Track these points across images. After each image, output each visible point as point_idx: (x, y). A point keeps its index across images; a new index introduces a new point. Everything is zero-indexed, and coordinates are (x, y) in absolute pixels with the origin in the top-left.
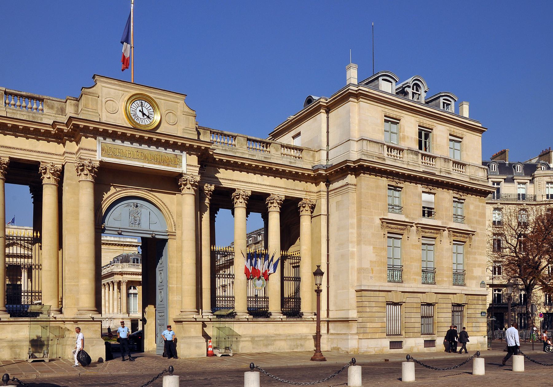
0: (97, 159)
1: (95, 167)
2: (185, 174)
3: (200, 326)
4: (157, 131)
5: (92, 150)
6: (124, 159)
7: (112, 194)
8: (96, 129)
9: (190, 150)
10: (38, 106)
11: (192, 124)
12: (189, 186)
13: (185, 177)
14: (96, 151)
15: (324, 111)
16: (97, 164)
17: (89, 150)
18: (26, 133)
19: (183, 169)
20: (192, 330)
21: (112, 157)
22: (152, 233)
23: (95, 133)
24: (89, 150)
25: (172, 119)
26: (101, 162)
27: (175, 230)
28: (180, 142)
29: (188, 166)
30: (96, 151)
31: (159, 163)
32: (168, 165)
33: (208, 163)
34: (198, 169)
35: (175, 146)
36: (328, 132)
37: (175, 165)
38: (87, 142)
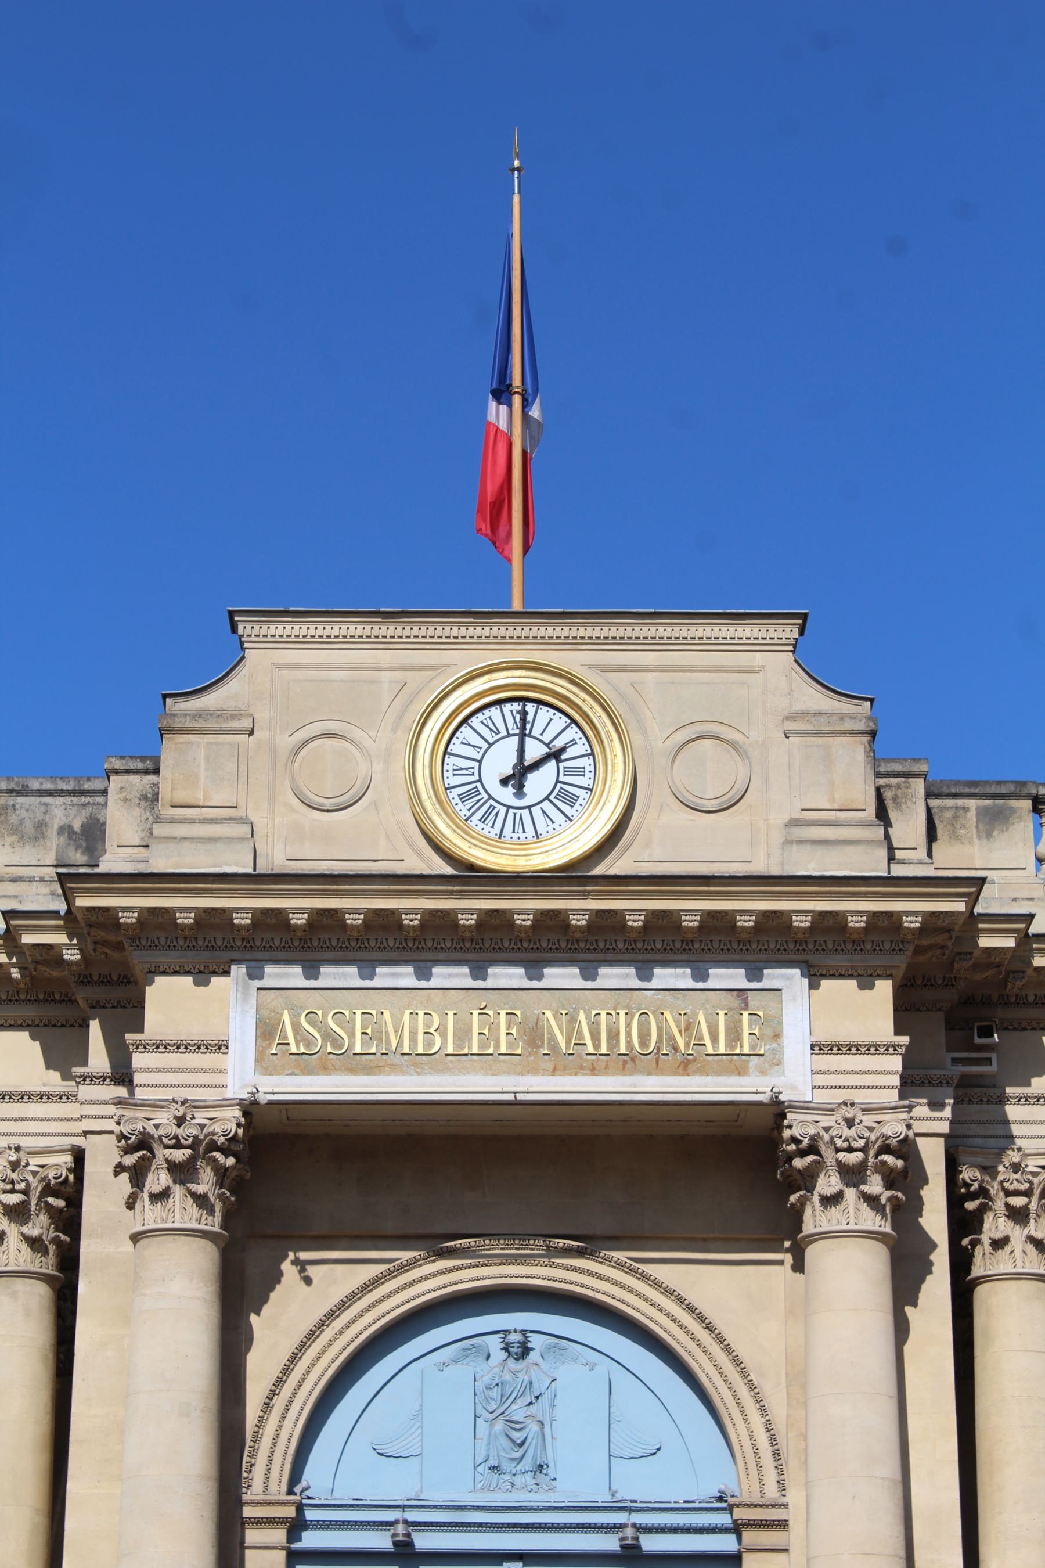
0: (230, 1095)
1: (213, 1146)
2: (794, 1106)
4: (613, 865)
5: (201, 1046)
6: (395, 1069)
7: (317, 1297)
8: (213, 921)
9: (824, 949)
11: (847, 774)
12: (829, 1183)
13: (799, 1126)
14: (222, 1046)
16: (228, 1122)
17: (180, 1046)
19: (791, 1075)
21: (325, 1068)
22: (620, 1518)
23: (213, 946)
24: (180, 1046)
25: (712, 773)
26: (250, 1109)
27: (782, 1486)
28: (747, 907)
29: (818, 1050)
30: (222, 1046)
31: (629, 1063)
32: (686, 1066)
34: (896, 1063)
35: (713, 942)
37: (734, 1063)
38: (171, 1002)
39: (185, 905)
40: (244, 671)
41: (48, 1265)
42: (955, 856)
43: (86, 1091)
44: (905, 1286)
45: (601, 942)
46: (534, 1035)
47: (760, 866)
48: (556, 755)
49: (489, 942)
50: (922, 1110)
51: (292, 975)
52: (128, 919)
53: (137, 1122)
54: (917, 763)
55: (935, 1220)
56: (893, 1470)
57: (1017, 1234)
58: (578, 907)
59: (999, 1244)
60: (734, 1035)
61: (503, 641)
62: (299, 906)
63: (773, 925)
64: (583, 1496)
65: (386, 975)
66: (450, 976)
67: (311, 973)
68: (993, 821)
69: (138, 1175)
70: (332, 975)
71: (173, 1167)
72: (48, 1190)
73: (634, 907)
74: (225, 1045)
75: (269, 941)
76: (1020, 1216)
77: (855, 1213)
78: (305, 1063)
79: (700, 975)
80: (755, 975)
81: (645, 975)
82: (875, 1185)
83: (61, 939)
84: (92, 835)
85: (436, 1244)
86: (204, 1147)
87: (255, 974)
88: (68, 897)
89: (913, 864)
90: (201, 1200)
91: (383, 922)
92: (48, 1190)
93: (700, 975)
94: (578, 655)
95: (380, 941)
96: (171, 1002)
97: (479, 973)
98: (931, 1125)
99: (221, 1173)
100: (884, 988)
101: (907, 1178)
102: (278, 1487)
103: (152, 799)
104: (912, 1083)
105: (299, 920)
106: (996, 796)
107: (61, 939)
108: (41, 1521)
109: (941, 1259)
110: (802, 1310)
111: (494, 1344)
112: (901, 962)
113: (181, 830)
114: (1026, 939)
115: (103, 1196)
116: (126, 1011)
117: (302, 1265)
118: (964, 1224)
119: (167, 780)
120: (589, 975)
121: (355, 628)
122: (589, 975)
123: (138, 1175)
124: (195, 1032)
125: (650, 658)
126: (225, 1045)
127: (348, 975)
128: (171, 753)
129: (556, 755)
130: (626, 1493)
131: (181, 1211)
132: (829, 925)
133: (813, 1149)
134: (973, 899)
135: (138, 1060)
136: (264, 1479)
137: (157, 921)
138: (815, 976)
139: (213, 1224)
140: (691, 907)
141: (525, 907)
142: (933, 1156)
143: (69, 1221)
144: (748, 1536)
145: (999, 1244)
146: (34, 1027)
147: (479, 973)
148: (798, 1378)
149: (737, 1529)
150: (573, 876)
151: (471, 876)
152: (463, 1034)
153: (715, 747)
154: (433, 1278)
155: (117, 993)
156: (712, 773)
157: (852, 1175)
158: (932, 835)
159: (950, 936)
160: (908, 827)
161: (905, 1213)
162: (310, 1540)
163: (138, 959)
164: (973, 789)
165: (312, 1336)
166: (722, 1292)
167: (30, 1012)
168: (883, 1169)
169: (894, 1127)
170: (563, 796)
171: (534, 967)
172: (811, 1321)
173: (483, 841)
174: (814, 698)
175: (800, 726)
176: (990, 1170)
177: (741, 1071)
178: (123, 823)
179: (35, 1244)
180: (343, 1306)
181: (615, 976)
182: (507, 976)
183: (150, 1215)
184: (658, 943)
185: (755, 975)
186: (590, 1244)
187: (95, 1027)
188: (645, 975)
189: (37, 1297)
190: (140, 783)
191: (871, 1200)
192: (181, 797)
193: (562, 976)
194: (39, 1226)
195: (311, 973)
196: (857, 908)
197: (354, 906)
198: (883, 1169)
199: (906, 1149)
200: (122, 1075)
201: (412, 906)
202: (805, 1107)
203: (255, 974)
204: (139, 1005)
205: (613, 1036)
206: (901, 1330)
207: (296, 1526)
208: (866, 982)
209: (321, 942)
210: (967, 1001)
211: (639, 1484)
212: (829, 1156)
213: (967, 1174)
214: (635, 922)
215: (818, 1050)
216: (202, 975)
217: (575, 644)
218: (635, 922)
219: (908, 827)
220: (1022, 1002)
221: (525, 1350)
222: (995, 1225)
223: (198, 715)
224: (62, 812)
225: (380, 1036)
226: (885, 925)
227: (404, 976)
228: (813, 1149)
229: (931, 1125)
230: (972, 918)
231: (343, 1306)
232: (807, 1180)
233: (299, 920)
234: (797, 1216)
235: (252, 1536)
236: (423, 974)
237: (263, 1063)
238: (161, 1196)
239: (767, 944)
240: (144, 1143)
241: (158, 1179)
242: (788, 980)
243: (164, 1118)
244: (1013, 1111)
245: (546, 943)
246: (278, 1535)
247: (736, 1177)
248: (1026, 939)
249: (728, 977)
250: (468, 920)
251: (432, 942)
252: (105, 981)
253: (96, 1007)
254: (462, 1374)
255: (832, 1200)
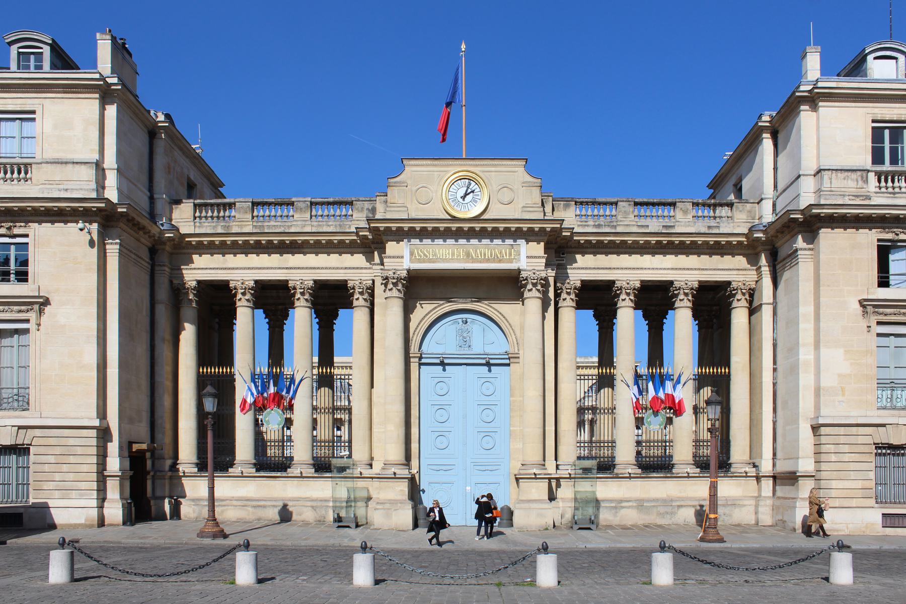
3: (544, 485)
4: (485, 217)
6: (439, 262)
7: (424, 311)
8: (400, 229)
9: (529, 235)
10: (335, 211)
11: (535, 196)
12: (530, 286)
13: (524, 274)
14: (402, 257)
15: (768, 135)
16: (404, 274)
18: (319, 247)
20: (533, 490)
21: (424, 262)
23: (400, 235)
25: (506, 196)
26: (409, 271)
28: (513, 226)
29: (528, 258)
30: (402, 257)
31: (488, 261)
32: (500, 261)
33: (561, 248)
34: (544, 260)
35: (506, 234)
36: (775, 169)
39: (394, 226)
40: (405, 172)
41: (368, 304)
42: (558, 215)
43: (374, 267)
44: (545, 309)
45: (482, 234)
46: (468, 254)
47: (516, 217)
48: (473, 192)
49: (458, 234)
50: (550, 271)
51: (417, 241)
52: (382, 229)
53: (385, 274)
54: (552, 195)
55: (551, 294)
56: (541, 346)
57: (568, 297)
58: (477, 226)
59: (564, 300)
60: (510, 254)
61: (461, 165)
62: (418, 226)
63: (519, 230)
64: (478, 352)
65: (437, 241)
66: (451, 242)
67: (421, 241)
68: (566, 207)
69: (386, 285)
70: (425, 241)
71: (393, 283)
72: (367, 288)
73: (489, 226)
74: (403, 257)
75: (412, 234)
76: (569, 294)
77: (535, 293)
78: (420, 261)
79: (503, 241)
80: (515, 241)
81: (492, 241)
82: (539, 287)
83: (368, 233)
84: (373, 210)
85: (448, 300)
86: (399, 279)
87: (409, 241)
88: (369, 224)
89: (549, 216)
90: (399, 290)
91: (436, 230)
92: (367, 288)
93: (503, 241)
94: (478, 168)
95: (435, 234)
96: (391, 247)
97: (456, 241)
98: (551, 273)
99: (403, 285)
100: (542, 244)
101: (546, 285)
102: (417, 350)
103: (386, 202)
104: (547, 265)
105: (418, 229)
106: (567, 201)
107: (368, 233)
108: (369, 357)
109: (552, 303)
110: (523, 314)
111: (460, 321)
112: (546, 238)
113: (393, 209)
114: (572, 233)
115: (379, 289)
116: (382, 250)
117: (421, 304)
118: (557, 295)
119: (389, 198)
120: (480, 241)
121: (429, 162)
122: (480, 241)
123: (386, 285)
124: (396, 254)
125: (493, 169)
126: (403, 257)
127: (428, 241)
128: (389, 191)
129: (473, 192)
130: (487, 351)
131: (395, 293)
132: (531, 230)
133: (526, 279)
134: (562, 224)
135: (385, 260)
136: (414, 348)
137: (388, 229)
138: (528, 242)
139: (402, 295)
140: (501, 226)
141: (466, 226)
142: (551, 280)
143: (372, 295)
144: (512, 360)
145: (564, 300)
146: (363, 253)
147: (456, 241)
148: (522, 328)
149: (509, 359)
150: (476, 219)
151: (454, 219)
152: (453, 254)
153: (506, 189)
154: (448, 307)
155: (380, 246)
156: (506, 196)
157: (534, 285)
158: (553, 210)
159: (557, 232)
160: (548, 208)
161: (545, 293)
162: (423, 361)
163: (384, 238)
164: (562, 200)
165: (423, 319)
166: (506, 310)
167: (362, 250)
168: (541, 284)
169: (543, 275)
170: (474, 201)
171: (468, 240)
172: (524, 315)
173: (457, 211)
174: (529, 178)
175: (525, 184)
176: (563, 284)
177: (512, 262)
178: (380, 207)
179: (365, 300)
180: (429, 313)
181: (486, 241)
182: (462, 241)
183: (388, 294)
184: (495, 234)
185: (515, 241)
186: (480, 300)
187: (376, 253)
188: (492, 241)
189: (367, 311)
190: (383, 198)
191: (538, 290)
192: (392, 201)
193: (474, 242)
194: (366, 296)
195: (421, 241)
196: (536, 226)
197: (430, 226)
198: (541, 284)
199: (546, 279)
200: (382, 264)
201: (442, 226)
202: (525, 270)
203: (409, 241)
204: (385, 248)
205: (485, 255)
206: (544, 318)
207: (420, 358)
208: (539, 243)
209: (423, 234)
210: (560, 247)
211: (490, 349)
212: (530, 281)
213: (558, 285)
214: (490, 229)
215: (528, 258)
216: (398, 241)
217: (477, 166)
218: (490, 229)
219: (548, 208)
220: (571, 247)
221: (467, 322)
222: (564, 295)
223: (395, 183)
224: (367, 205)
225: (435, 255)
226: (542, 230)
227: (440, 241)
228: (526, 279)
229: (551, 273)
230: (561, 229)
231: (429, 313)
232: (525, 286)
233: (418, 229)
234: (523, 294)
235: (412, 360)
236: (445, 241)
237: (411, 261)
238: (391, 289)
239: (517, 234)
240: (387, 278)
241: (390, 286)
242: (522, 242)
243: (391, 273)
244: (569, 271)
245: (471, 234)
246: (417, 360)
247: (509, 285)
248: (572, 233)
249: (509, 242)
250: (454, 229)
251: (447, 234)
252: (377, 243)
253: (376, 249)
254: (454, 326)
255: (530, 290)
